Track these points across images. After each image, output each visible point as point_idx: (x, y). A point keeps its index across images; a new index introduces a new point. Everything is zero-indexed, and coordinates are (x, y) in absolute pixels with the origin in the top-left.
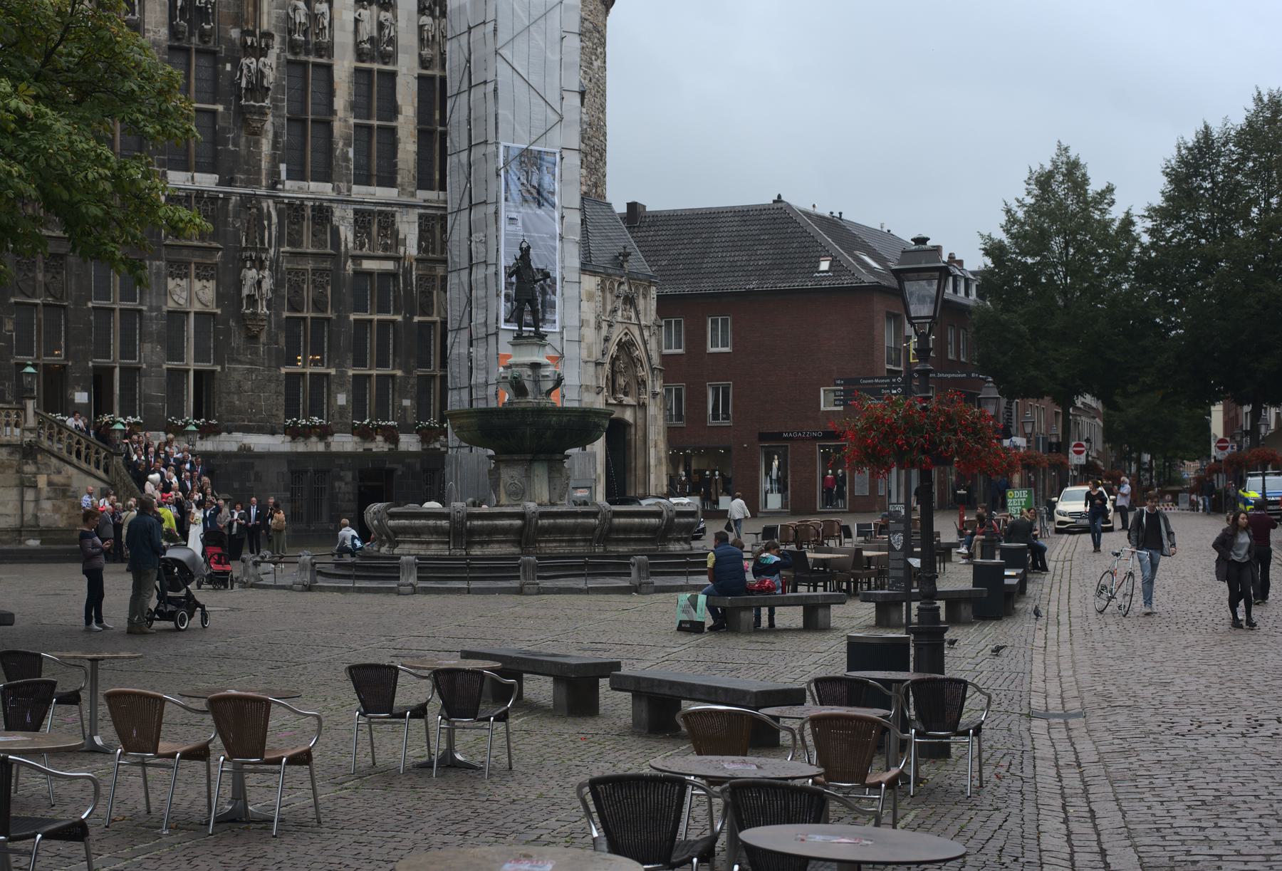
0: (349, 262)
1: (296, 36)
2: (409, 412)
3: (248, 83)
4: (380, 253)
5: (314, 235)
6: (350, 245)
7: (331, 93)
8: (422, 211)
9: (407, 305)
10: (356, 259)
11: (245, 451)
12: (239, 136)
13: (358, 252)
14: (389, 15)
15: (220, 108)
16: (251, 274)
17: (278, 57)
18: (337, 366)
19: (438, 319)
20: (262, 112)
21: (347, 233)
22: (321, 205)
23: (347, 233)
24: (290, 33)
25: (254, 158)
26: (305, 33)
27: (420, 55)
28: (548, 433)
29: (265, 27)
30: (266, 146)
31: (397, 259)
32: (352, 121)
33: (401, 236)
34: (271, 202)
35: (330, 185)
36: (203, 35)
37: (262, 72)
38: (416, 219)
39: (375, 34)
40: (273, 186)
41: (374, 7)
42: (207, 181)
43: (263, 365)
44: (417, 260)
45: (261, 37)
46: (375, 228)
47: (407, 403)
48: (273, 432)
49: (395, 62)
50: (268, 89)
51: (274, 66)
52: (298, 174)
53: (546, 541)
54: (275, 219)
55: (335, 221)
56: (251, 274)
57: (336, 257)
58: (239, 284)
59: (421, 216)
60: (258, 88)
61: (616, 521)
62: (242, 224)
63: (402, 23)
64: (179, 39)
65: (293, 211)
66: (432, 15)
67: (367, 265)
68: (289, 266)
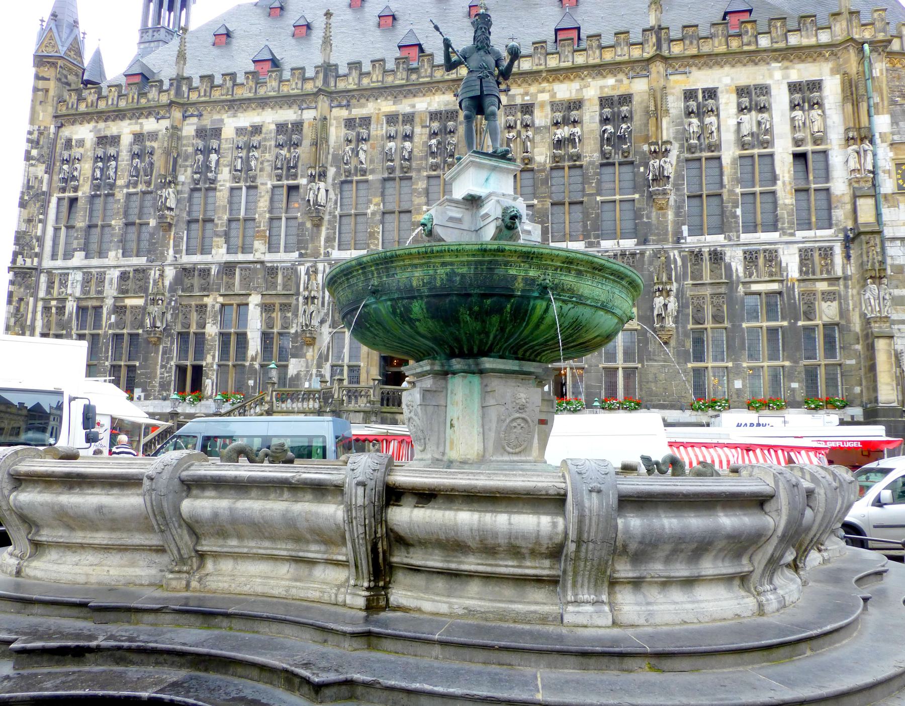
0: (741, 286)
1: (692, 141)
2: (797, 393)
4: (767, 279)
5: (711, 271)
6: (741, 274)
7: (721, 174)
8: (801, 245)
9: (792, 313)
10: (744, 283)
12: (651, 212)
13: (748, 280)
14: (766, 115)
15: (637, 196)
16: (659, 301)
17: (678, 157)
18: (734, 360)
19: (820, 322)
21: (738, 267)
22: (715, 251)
23: (738, 267)
25: (663, 226)
27: (794, 138)
28: (417, 308)
29: (665, 138)
30: (671, 215)
31: (782, 281)
32: (738, 190)
33: (784, 264)
34: (676, 252)
35: (723, 236)
36: (626, 153)
38: (797, 251)
39: (755, 129)
40: (678, 242)
41: (753, 113)
42: (629, 244)
44: (798, 280)
46: (761, 261)
47: (795, 385)
48: (682, 408)
49: (773, 146)
50: (668, 177)
51: (674, 163)
52: (697, 230)
53: (236, 556)
54: (679, 262)
55: (727, 259)
56: (659, 301)
57: (731, 284)
58: (652, 309)
59: (800, 251)
60: (660, 177)
61: (404, 516)
62: (655, 268)
63: (777, 118)
64: (607, 158)
65: (697, 256)
66: (802, 109)
67: (755, 288)
68: (692, 293)
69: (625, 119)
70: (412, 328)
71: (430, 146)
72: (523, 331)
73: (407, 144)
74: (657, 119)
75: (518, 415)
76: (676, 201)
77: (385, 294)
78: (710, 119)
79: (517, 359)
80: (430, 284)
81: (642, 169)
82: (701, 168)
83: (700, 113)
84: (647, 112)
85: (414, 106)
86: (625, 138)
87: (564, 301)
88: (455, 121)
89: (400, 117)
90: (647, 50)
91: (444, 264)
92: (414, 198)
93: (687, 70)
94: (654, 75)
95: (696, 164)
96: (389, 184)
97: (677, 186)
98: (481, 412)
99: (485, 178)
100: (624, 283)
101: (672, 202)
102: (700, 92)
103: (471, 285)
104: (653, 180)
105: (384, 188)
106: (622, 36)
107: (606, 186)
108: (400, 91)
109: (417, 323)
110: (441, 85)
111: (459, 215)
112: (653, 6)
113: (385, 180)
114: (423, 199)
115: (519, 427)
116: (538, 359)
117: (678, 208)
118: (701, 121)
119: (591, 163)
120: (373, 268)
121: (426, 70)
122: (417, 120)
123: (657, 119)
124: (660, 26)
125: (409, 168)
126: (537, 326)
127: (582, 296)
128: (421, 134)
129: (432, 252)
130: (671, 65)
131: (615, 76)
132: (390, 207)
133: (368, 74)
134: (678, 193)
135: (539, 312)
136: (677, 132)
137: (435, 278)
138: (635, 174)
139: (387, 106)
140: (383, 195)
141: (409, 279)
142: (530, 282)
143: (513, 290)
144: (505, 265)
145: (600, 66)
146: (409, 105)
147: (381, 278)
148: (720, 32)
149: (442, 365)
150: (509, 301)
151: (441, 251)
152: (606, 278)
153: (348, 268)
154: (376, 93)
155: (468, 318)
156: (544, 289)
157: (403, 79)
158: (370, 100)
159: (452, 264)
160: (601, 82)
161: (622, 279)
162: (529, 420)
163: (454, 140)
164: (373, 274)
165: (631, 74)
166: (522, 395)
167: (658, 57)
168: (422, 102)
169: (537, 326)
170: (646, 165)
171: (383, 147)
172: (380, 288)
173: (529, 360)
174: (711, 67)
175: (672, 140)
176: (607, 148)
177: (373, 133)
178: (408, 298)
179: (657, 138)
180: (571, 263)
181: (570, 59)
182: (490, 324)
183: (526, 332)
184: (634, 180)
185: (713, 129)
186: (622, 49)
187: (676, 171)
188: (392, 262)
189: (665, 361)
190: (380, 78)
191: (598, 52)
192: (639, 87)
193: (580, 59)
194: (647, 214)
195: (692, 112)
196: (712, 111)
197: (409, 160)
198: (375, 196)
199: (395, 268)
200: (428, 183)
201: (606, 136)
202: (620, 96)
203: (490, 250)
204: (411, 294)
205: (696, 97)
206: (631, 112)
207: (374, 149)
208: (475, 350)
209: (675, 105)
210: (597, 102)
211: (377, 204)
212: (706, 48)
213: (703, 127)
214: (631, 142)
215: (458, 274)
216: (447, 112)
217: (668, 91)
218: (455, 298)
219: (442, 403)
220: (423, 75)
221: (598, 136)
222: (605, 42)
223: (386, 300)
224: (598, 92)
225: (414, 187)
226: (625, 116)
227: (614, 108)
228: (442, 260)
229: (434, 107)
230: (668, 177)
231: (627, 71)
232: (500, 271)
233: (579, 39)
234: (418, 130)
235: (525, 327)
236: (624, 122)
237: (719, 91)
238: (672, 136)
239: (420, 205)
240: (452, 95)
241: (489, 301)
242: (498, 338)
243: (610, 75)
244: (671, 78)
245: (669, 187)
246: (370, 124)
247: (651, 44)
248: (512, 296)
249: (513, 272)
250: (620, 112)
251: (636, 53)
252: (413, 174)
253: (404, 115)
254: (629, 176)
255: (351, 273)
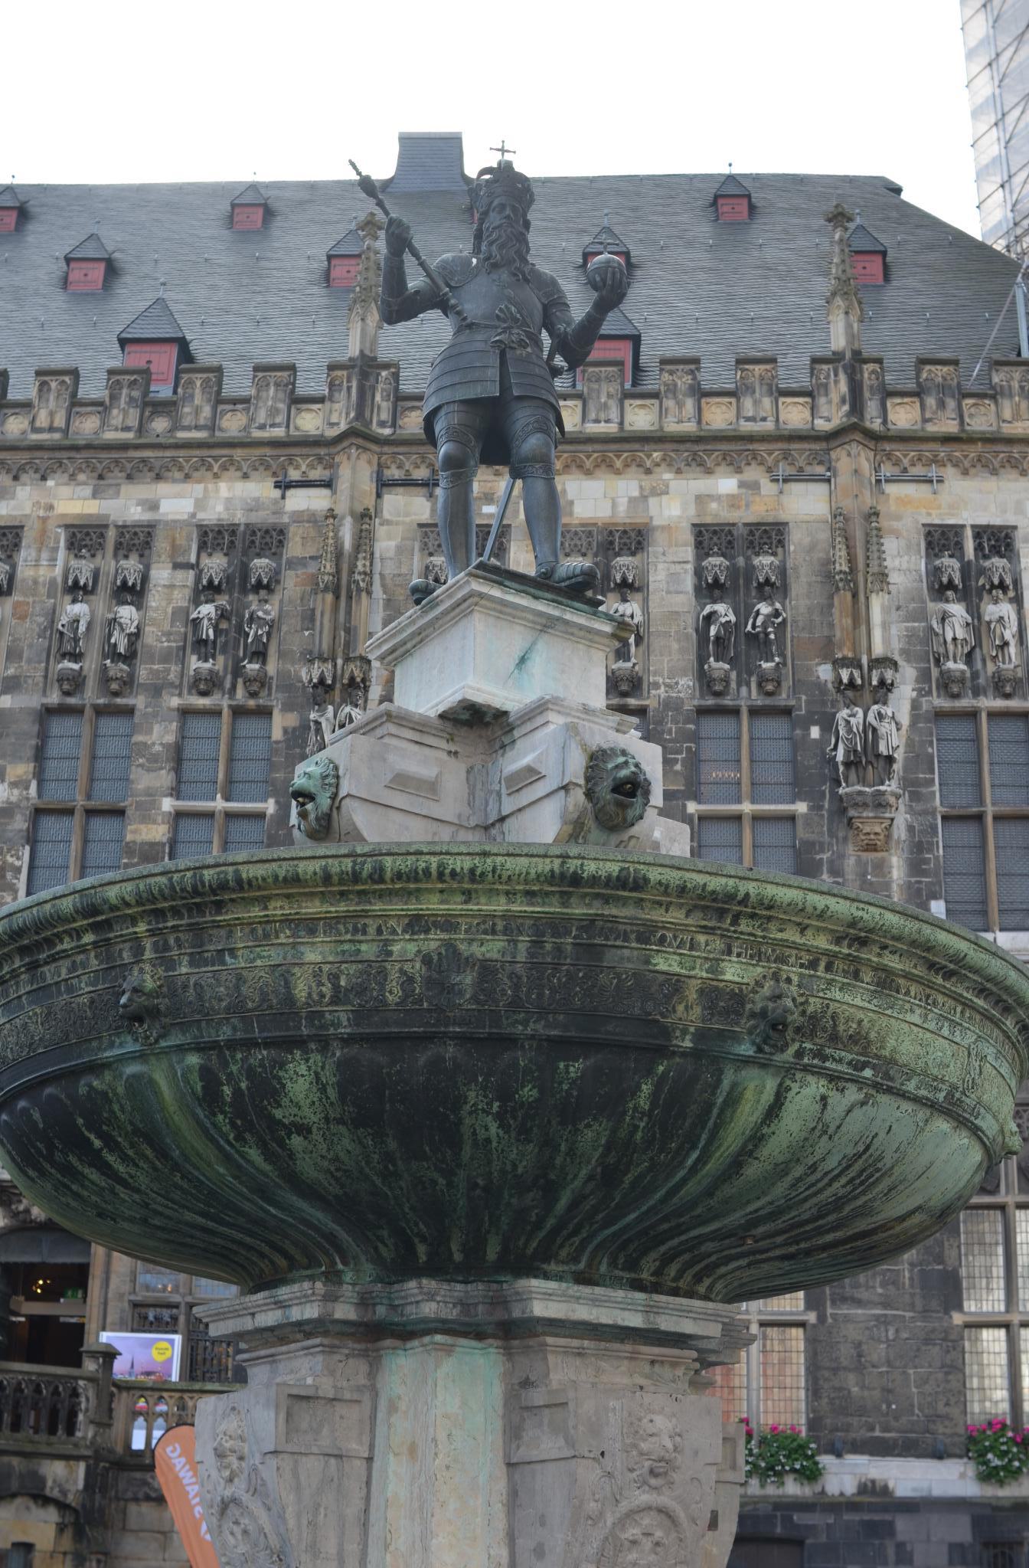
1: (951, 665)
3: (847, 752)
11: (874, 1493)
12: (842, 856)
15: (801, 807)
17: (915, 705)
20: (880, 803)
24: (937, 661)
26: (969, 658)
28: (302, 1082)
29: (878, 650)
30: (897, 868)
36: (769, 684)
37: (875, 730)
43: (912, 1307)
45: (870, 670)
51: (905, 720)
60: (868, 758)
69: (767, 589)
70: (269, 1156)
71: (196, 623)
72: (684, 1181)
73: (127, 613)
74: (855, 595)
75: (645, 1498)
76: (910, 829)
77: (183, 1027)
78: (999, 610)
79: (638, 1286)
80: (361, 992)
81: (815, 732)
82: (977, 739)
83: (971, 589)
84: (828, 576)
85: (154, 506)
86: (767, 642)
87: (833, 1078)
88: (276, 556)
89: (111, 534)
90: (824, 410)
91: (417, 924)
92: (135, 773)
93: (933, 472)
94: (844, 478)
95: (963, 729)
96: (59, 726)
97: (914, 789)
98: (501, 1485)
99: (517, 655)
100: (1009, 1023)
101: (900, 831)
102: (969, 533)
103: (515, 1004)
104: (847, 764)
105: (43, 736)
106: (758, 369)
107: (714, 773)
108: (117, 462)
109: (296, 1141)
110: (238, 453)
111: (428, 772)
112: (839, 301)
113: (49, 711)
114: (165, 778)
115: (647, 1544)
116: (702, 1289)
117: (919, 849)
118: (975, 611)
119: (668, 704)
120: (142, 928)
121: (197, 411)
122: (161, 544)
123: (855, 595)
124: (857, 353)
125: (128, 683)
126: (736, 1164)
127: (892, 1061)
128: (172, 587)
129: (378, 876)
130: (889, 456)
131: (739, 470)
132: (57, 794)
133: (26, 405)
134: (918, 807)
135: (747, 1114)
136: (911, 636)
137: (383, 973)
138: (798, 745)
139: (73, 500)
140: (40, 756)
141: (283, 973)
142: (726, 1003)
143: (666, 1032)
144: (643, 939)
145: (698, 440)
146: (141, 503)
147: (170, 964)
148: (1016, 385)
149: (365, 1302)
150: (649, 1072)
151: (413, 876)
152: (967, 1005)
153: (40, 925)
154: (43, 459)
155: (494, 1128)
156: (774, 1029)
157: (127, 429)
158: (24, 477)
159: (448, 924)
160: (699, 484)
161: (1007, 1010)
162: (682, 1516)
163: (270, 610)
164: (138, 951)
165: (784, 469)
166: (661, 1423)
167: (853, 430)
168: (179, 496)
169: (736, 1164)
170: (828, 724)
171: (52, 615)
172: (163, 1003)
173: (675, 1292)
174: (994, 472)
175: (897, 657)
176: (717, 667)
177: (24, 572)
178: (268, 1044)
179: (855, 647)
180: (863, 942)
181: (614, 414)
182: (571, 1152)
183: (692, 1188)
184: (794, 762)
185: (1008, 635)
186: (757, 403)
187: (910, 744)
188: (219, 906)
189: (886, 1305)
190: (60, 421)
191: (690, 404)
192: (805, 505)
193: (641, 418)
194: (831, 862)
195: (950, 585)
196: (1002, 586)
197: (130, 657)
198: (16, 758)
199: (230, 927)
200: (182, 728)
201: (713, 630)
202: (753, 527)
203: (594, 880)
204: (285, 1027)
205: (959, 546)
206: (783, 572)
207: (23, 618)
208: (492, 1253)
209: (903, 562)
210: (689, 537)
211: (20, 784)
212: (981, 419)
213: (978, 625)
214: (782, 655)
215: (469, 962)
216: (252, 530)
217: (884, 523)
218: (450, 1051)
219: (357, 1447)
220: (186, 422)
221: (691, 631)
222: (708, 378)
223: (181, 1049)
224: (692, 511)
225: (138, 738)
226: (767, 581)
227: (734, 557)
228: (413, 907)
229: (215, 512)
230: (890, 760)
231: (770, 460)
232: (624, 957)
233: (637, 368)
234: (161, 574)
235: (694, 1170)
236: (763, 598)
237: (1019, 535)
238: (896, 645)
239: (152, 795)
240: (270, 483)
241: (575, 1069)
242: (587, 1206)
243: (722, 468)
244: (891, 489)
245: (891, 786)
246: (17, 546)
247: (835, 397)
248: (663, 1051)
249: (666, 963)
250: (750, 569)
251: (795, 415)
252: (139, 701)
253: (123, 529)
254: (783, 749)
255: (49, 942)
